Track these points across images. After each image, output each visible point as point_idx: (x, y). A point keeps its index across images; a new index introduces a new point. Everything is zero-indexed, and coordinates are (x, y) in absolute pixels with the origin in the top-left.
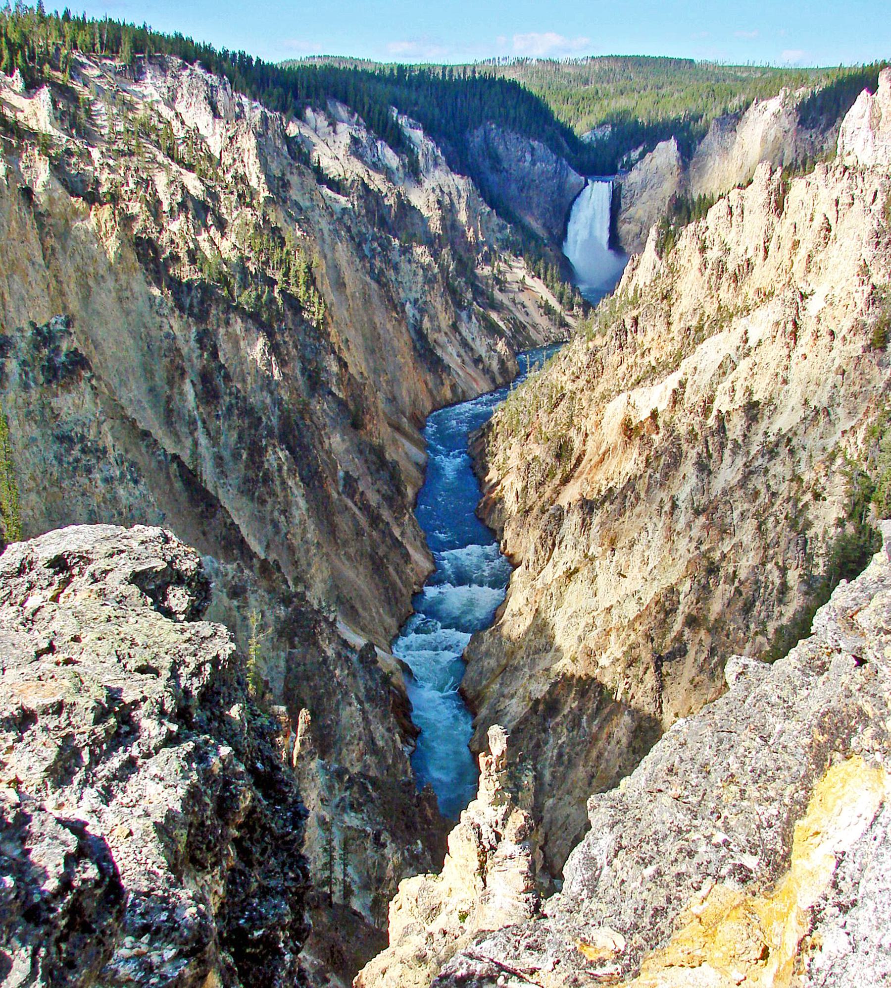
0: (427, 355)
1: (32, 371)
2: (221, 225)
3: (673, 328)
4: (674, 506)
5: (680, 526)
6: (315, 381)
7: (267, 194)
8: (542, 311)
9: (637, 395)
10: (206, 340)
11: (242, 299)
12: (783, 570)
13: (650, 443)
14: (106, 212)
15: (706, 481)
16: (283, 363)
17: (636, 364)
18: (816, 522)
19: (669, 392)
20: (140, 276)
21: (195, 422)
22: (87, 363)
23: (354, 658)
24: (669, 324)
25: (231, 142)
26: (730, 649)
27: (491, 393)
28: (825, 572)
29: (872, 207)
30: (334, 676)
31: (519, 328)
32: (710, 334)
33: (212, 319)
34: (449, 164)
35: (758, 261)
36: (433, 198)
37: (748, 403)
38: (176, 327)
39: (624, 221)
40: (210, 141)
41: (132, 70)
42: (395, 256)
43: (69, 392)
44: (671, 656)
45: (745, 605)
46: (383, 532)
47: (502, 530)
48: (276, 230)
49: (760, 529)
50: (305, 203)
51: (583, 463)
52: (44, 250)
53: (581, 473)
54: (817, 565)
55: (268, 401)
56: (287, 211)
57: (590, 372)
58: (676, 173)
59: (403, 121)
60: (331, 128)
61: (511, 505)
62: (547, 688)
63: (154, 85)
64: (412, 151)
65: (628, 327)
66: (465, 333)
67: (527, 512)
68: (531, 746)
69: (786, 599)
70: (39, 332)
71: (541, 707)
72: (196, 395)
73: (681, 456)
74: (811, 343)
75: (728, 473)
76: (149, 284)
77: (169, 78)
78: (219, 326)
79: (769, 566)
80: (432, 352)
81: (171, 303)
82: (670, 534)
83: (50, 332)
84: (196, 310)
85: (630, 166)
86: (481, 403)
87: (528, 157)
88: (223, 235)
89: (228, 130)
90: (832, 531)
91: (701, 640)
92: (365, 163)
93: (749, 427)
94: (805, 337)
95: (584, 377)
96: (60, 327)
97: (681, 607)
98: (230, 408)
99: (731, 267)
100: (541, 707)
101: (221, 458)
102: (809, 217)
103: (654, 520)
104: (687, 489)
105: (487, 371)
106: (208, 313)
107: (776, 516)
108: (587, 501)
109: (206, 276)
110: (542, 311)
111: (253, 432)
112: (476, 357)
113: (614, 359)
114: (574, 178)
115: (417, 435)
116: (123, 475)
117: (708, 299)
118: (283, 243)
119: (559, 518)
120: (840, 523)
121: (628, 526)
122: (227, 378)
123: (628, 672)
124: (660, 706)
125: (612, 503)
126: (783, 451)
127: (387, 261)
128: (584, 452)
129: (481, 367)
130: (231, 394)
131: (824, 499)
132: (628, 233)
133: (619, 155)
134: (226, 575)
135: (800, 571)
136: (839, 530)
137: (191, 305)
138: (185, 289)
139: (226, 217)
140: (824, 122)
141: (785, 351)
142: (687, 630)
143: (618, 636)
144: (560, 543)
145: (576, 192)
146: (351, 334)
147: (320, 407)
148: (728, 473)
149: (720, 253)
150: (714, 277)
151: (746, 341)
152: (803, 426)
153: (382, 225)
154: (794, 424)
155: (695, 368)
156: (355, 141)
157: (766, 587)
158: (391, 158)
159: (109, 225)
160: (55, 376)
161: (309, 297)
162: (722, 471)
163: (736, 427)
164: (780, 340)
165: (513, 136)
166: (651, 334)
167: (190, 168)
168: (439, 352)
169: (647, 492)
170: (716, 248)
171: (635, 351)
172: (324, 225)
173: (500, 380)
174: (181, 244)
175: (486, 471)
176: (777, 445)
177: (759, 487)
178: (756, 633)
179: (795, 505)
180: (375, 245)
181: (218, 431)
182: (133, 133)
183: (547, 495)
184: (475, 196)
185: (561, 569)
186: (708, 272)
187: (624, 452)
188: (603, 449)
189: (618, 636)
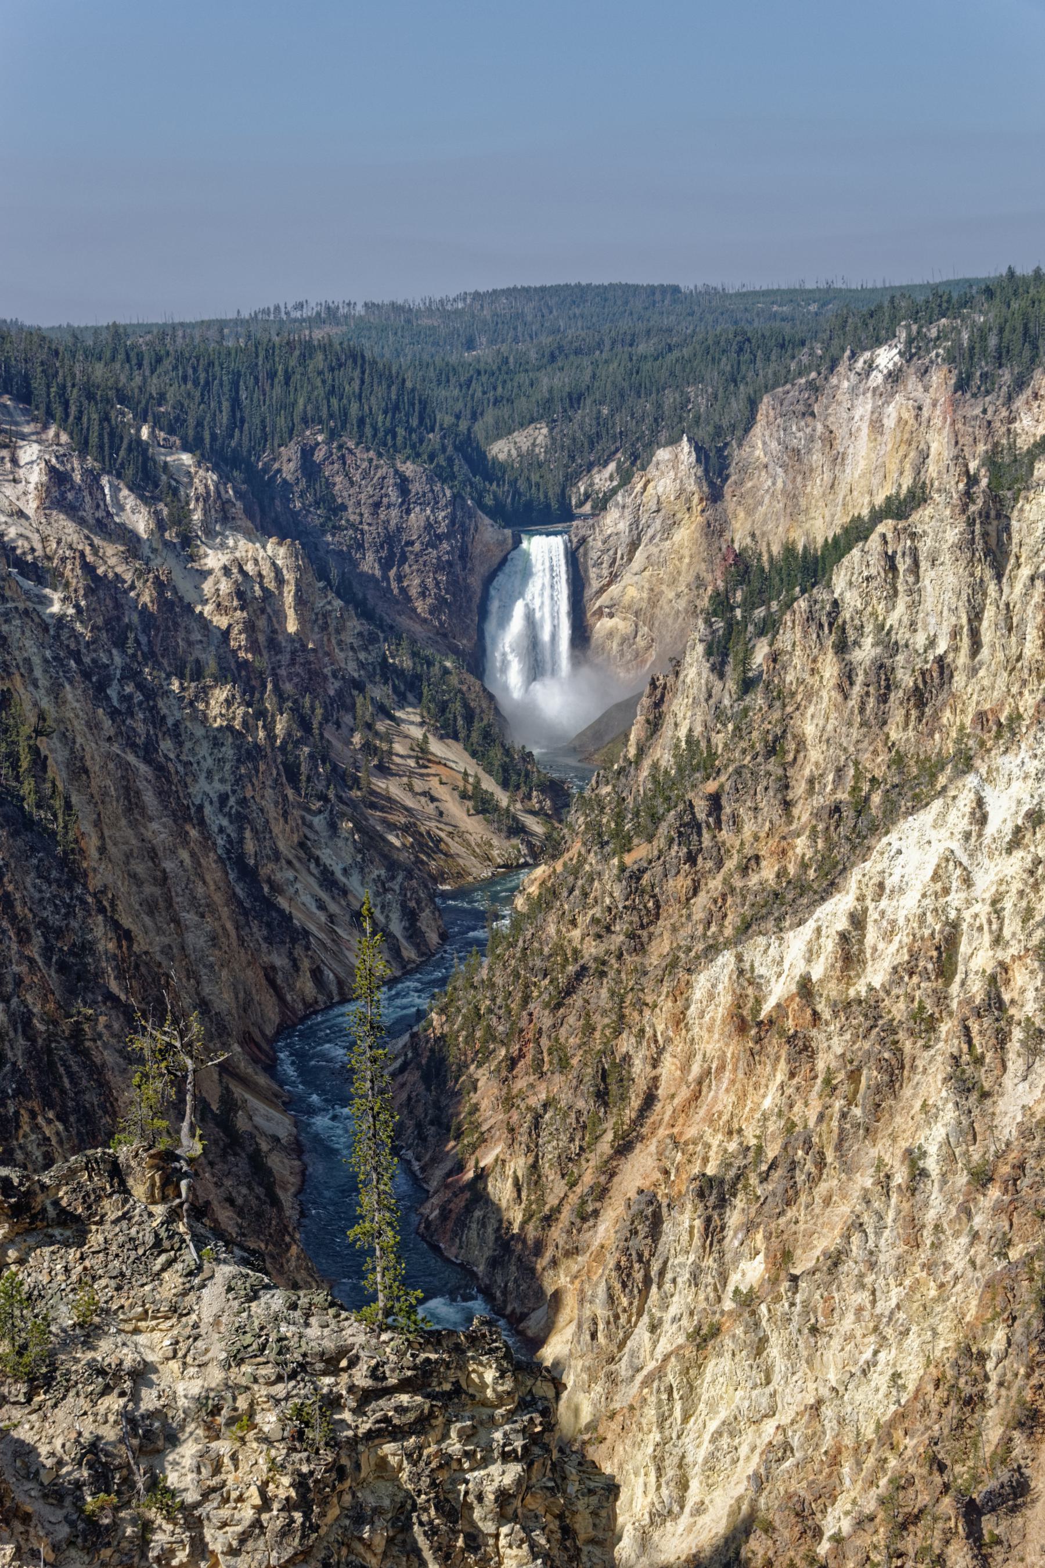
0: (259, 907)
3: (796, 812)
8: (470, 804)
9: (759, 952)
13: (802, 1050)
15: (976, 1112)
17: (732, 890)
24: (787, 805)
32: (892, 814)
34: (249, 513)
39: (599, 613)
58: (697, 508)
65: (701, 816)
66: (326, 855)
87: (394, 496)
92: (82, 522)
99: (906, 679)
103: (876, 1205)
104: (939, 1132)
114: (489, 532)
115: (262, 1080)
117: (865, 744)
119: (651, 1218)
127: (157, 719)
133: (571, 479)
143: (859, 1464)
144: (662, 1273)
145: (496, 560)
150: (871, 702)
151: (982, 820)
155: (881, 886)
156: (57, 478)
166: (748, 829)
168: (283, 903)
169: (838, 1147)
170: (868, 641)
171: (720, 864)
173: (409, 953)
183: (588, 1179)
184: (310, 577)
186: (857, 690)
188: (696, 1070)
189: (859, 1464)
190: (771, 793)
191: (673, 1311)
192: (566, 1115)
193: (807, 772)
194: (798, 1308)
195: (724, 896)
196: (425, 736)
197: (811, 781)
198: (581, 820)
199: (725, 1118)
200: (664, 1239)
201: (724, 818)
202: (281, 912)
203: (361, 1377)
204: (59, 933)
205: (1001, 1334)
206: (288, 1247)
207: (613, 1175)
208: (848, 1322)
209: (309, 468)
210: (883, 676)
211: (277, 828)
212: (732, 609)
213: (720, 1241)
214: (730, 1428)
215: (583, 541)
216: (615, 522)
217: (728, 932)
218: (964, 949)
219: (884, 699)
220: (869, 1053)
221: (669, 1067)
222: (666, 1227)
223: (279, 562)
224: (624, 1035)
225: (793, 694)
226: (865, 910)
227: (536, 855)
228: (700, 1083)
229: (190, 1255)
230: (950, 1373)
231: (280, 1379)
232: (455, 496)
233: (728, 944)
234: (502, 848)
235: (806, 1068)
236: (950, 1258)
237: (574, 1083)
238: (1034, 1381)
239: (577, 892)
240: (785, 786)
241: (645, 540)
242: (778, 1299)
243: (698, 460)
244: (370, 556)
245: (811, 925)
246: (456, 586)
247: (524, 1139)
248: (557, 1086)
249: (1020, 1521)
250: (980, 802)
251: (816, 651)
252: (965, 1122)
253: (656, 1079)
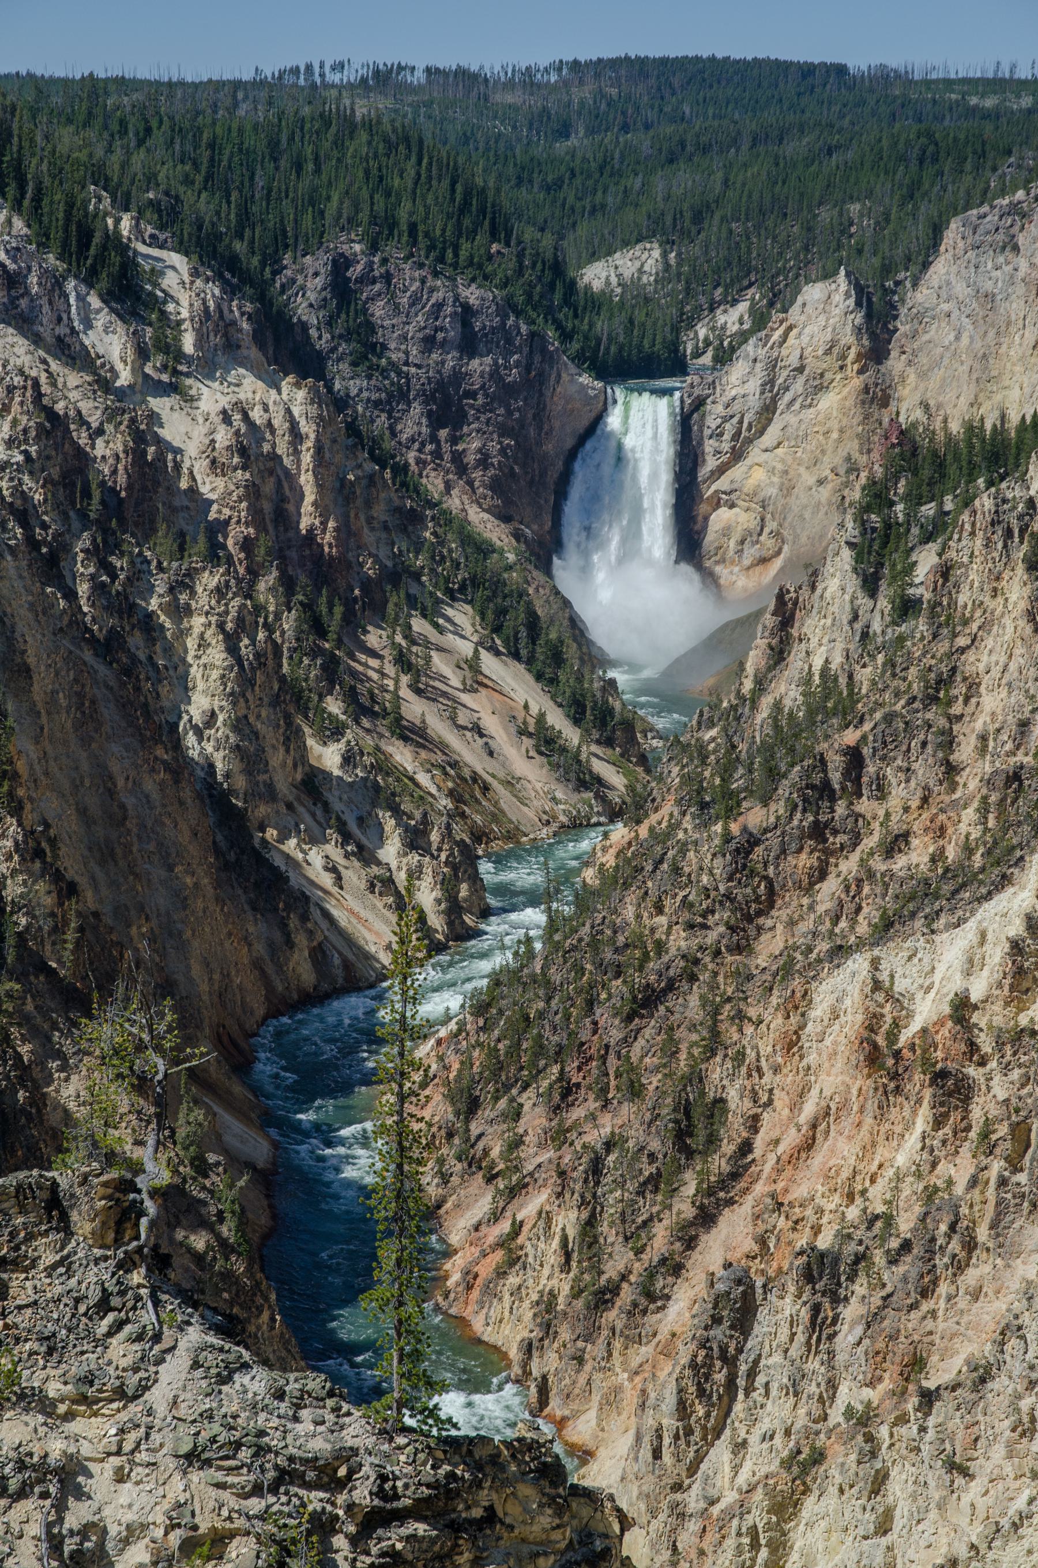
8: (528, 742)
13: (953, 1091)
17: (871, 875)
36: (223, 437)
58: (852, 369)
65: (835, 777)
92: (37, 340)
108: (822, 1255)
113: (805, 861)
115: (238, 1089)
128: (754, 1123)
166: (898, 794)
171: (856, 839)
188: (809, 1109)
190: (930, 749)
191: (765, 1425)
192: (635, 1158)
193: (979, 725)
194: (931, 1435)
195: (859, 882)
196: (476, 651)
197: (983, 738)
198: (676, 770)
199: (845, 1174)
200: (757, 1329)
201: (865, 779)
203: (362, 1494)
206: (260, 1310)
207: (690, 1243)
208: (993, 1459)
209: (342, 289)
211: (277, 758)
212: (892, 504)
213: (831, 1337)
215: (699, 403)
216: (741, 383)
217: (863, 928)
222: (762, 1314)
223: (296, 411)
224: (718, 1059)
225: (966, 622)
227: (614, 814)
228: (814, 1127)
229: (148, 1316)
231: (257, 1490)
232: (532, 335)
233: (861, 944)
234: (568, 801)
235: (955, 1117)
237: (648, 1116)
239: (665, 866)
240: (948, 742)
241: (781, 405)
242: (902, 1419)
243: (858, 304)
244: (417, 409)
245: (971, 925)
246: (525, 452)
247: (578, 1187)
248: (623, 1119)
251: (999, 566)
253: (756, 1118)
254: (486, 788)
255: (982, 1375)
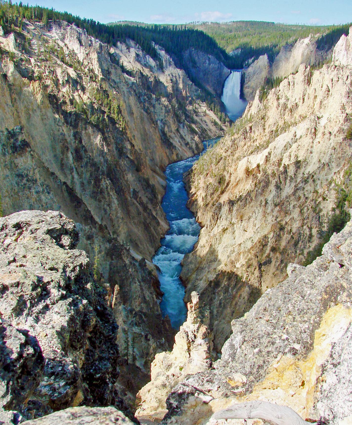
0: (166, 142)
1: (7, 148)
2: (83, 89)
3: (266, 131)
4: (266, 203)
5: (269, 211)
6: (121, 152)
7: (102, 77)
8: (213, 124)
9: (251, 158)
10: (77, 136)
11: (92, 119)
12: (310, 229)
13: (256, 177)
14: (37, 84)
15: (279, 193)
16: (108, 145)
17: (251, 145)
18: (324, 209)
19: (264, 157)
20: (50, 110)
21: (72, 169)
22: (30, 146)
23: (137, 264)
24: (264, 129)
25: (87, 56)
26: (289, 261)
27: (192, 157)
28: (327, 229)
29: (346, 82)
30: (129, 271)
31: (204, 131)
32: (281, 133)
33: (80, 127)
34: (175, 65)
35: (300, 104)
36: (169, 78)
37: (296, 161)
38: (65, 130)
39: (246, 88)
40: (79, 55)
41: (47, 26)
42: (153, 102)
43: (22, 157)
44: (265, 263)
45: (295, 243)
46: (149, 213)
47: (197, 212)
48: (105, 91)
49: (301, 212)
50: (117, 80)
51: (230, 185)
52: (12, 99)
53: (229, 189)
54: (324, 227)
55: (102, 160)
56: (110, 84)
57: (232, 149)
58: (267, 68)
59: (157, 47)
60: (128, 50)
61: (200, 202)
62: (215, 276)
63: (56, 33)
64: (160, 59)
65: (248, 131)
67: (207, 205)
68: (208, 300)
69: (311, 241)
70: (9, 132)
71: (213, 284)
72: (73, 158)
73: (269, 183)
74: (322, 137)
75: (288, 190)
76: (54, 113)
77: (62, 30)
78: (82, 130)
79: (305, 227)
80: (169, 141)
81: (63, 121)
82: (265, 214)
83: (14, 132)
84: (73, 124)
85: (248, 66)
86: (188, 161)
87: (207, 62)
88: (84, 93)
89: (86, 51)
90: (330, 213)
91: (277, 257)
92: (141, 64)
93: (296, 171)
94: (319, 135)
95: (230, 151)
96: (18, 130)
97: (269, 244)
98: (87, 163)
99: (289, 106)
100: (213, 284)
101: (83, 183)
102: (321, 86)
103: (258, 208)
105: (191, 148)
106: (78, 125)
107: (307, 207)
109: (77, 110)
110: (213, 124)
111: (96, 173)
112: (186, 142)
113: (242, 143)
114: (226, 70)
115: (162, 174)
116: (43, 191)
117: (280, 119)
118: (108, 97)
119: (220, 208)
120: (333, 210)
121: (248, 211)
122: (86, 151)
123: (248, 270)
124: (261, 284)
125: (241, 202)
126: (310, 180)
127: (150, 104)
128: (230, 181)
129: (188, 146)
130: (87, 157)
131: (327, 200)
132: (248, 92)
133: (244, 61)
134: (85, 231)
135: (317, 229)
136: (333, 212)
137: (71, 122)
138: (69, 115)
139: (85, 86)
140: (327, 47)
141: (311, 140)
142: (271, 253)
144: (220, 218)
146: (136, 133)
147: (123, 163)
148: (288, 190)
149: (285, 101)
150: (282, 110)
151: (295, 136)
152: (318, 171)
153: (148, 89)
154: (315, 169)
155: (275, 147)
156: (137, 55)
157: (304, 236)
158: (152, 62)
159: (38, 89)
160: (16, 150)
161: (119, 118)
162: (286, 189)
163: (291, 171)
164: (309, 136)
165: (201, 53)
166: (257, 133)
167: (71, 66)
168: (171, 141)
169: (255, 197)
170: (283, 99)
171: (250, 140)
172: (125, 89)
173: (196, 152)
174: (67, 97)
175: (190, 188)
176: (308, 178)
177: (301, 195)
178: (300, 254)
179: (315, 202)
180: (146, 97)
181: (82, 173)
182: (48, 52)
183: (215, 198)
184: (186, 77)
185: (220, 229)
186: (280, 108)
187: (246, 181)
189: (244, 255)
200: (222, 211)
202: (171, 143)
204: (119, 144)
205: (272, 234)
210: (285, 106)
214: (226, 247)
215: (244, 73)
218: (283, 162)
219: (285, 110)
220: (263, 180)
221: (233, 178)
226: (271, 152)
230: (262, 240)
236: (268, 219)
238: (276, 243)
249: (269, 268)
250: (295, 133)
252: (277, 194)
254: (206, 130)
255: (249, 218)
